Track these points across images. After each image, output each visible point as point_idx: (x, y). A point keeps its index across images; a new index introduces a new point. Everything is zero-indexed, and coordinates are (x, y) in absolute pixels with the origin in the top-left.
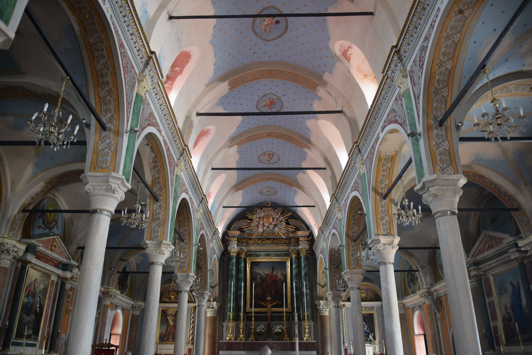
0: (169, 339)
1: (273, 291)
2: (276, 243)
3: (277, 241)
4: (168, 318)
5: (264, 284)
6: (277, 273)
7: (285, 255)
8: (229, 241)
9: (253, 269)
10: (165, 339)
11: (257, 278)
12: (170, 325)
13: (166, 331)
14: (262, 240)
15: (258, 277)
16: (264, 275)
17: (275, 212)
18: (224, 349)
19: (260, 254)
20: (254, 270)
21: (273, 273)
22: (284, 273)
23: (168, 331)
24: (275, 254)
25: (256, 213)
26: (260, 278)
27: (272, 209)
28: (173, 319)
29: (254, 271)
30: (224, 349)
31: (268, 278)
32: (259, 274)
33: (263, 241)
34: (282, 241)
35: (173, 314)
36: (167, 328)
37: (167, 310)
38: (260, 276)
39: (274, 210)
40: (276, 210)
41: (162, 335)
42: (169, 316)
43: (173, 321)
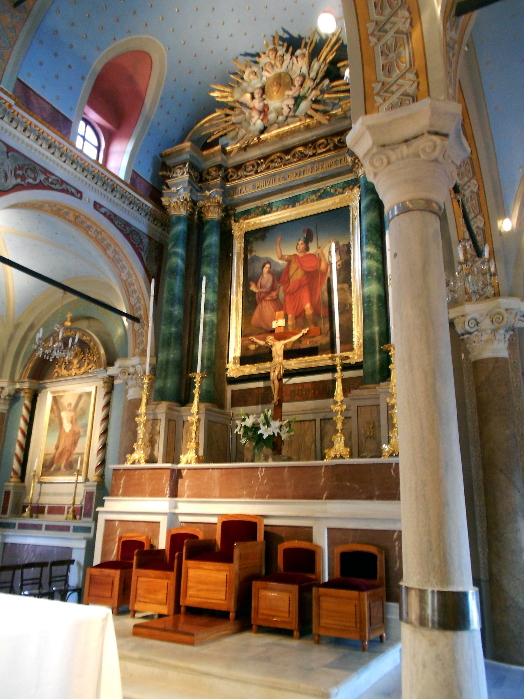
0: (59, 469)
1: (308, 306)
2: (311, 156)
3: (315, 148)
4: (63, 414)
5: (282, 288)
6: (319, 248)
7: (344, 188)
8: (169, 178)
9: (251, 251)
10: (52, 469)
11: (262, 273)
12: (65, 432)
13: (57, 448)
14: (268, 160)
15: (266, 270)
16: (281, 262)
17: (297, 57)
18: (121, 491)
19: (270, 205)
20: (253, 254)
21: (307, 249)
22: (341, 244)
23: (60, 450)
24: (314, 192)
25: (240, 81)
26: (269, 272)
27: (287, 51)
28: (72, 418)
29: (255, 256)
30: (121, 491)
31: (294, 266)
32: (268, 262)
33: (272, 161)
34: (328, 144)
35: (73, 405)
36: (59, 439)
37: (61, 397)
38: (270, 268)
39: (293, 54)
40: (298, 52)
41: (48, 457)
42: (64, 409)
43: (72, 422)
